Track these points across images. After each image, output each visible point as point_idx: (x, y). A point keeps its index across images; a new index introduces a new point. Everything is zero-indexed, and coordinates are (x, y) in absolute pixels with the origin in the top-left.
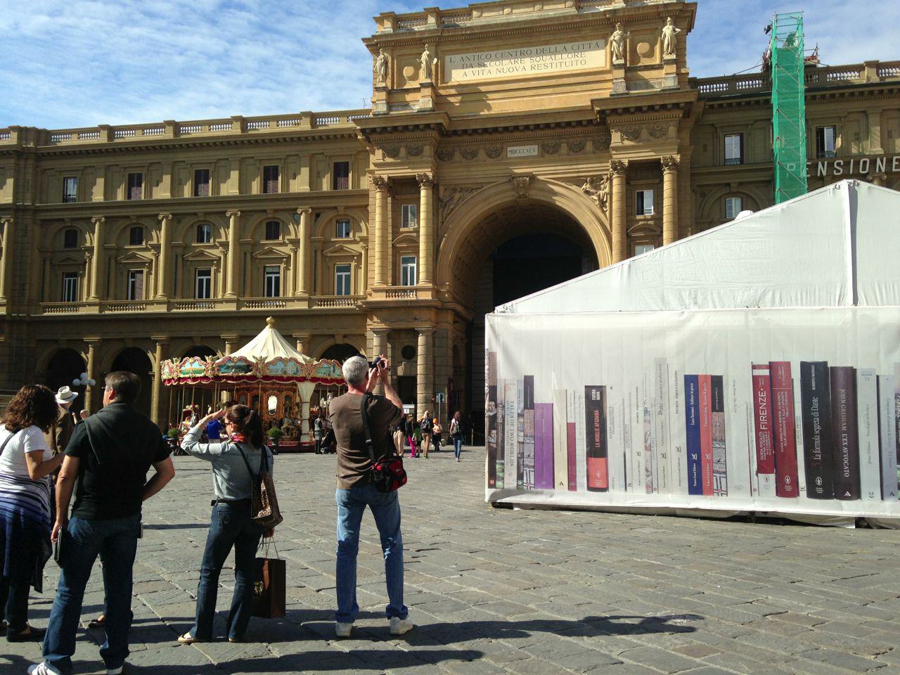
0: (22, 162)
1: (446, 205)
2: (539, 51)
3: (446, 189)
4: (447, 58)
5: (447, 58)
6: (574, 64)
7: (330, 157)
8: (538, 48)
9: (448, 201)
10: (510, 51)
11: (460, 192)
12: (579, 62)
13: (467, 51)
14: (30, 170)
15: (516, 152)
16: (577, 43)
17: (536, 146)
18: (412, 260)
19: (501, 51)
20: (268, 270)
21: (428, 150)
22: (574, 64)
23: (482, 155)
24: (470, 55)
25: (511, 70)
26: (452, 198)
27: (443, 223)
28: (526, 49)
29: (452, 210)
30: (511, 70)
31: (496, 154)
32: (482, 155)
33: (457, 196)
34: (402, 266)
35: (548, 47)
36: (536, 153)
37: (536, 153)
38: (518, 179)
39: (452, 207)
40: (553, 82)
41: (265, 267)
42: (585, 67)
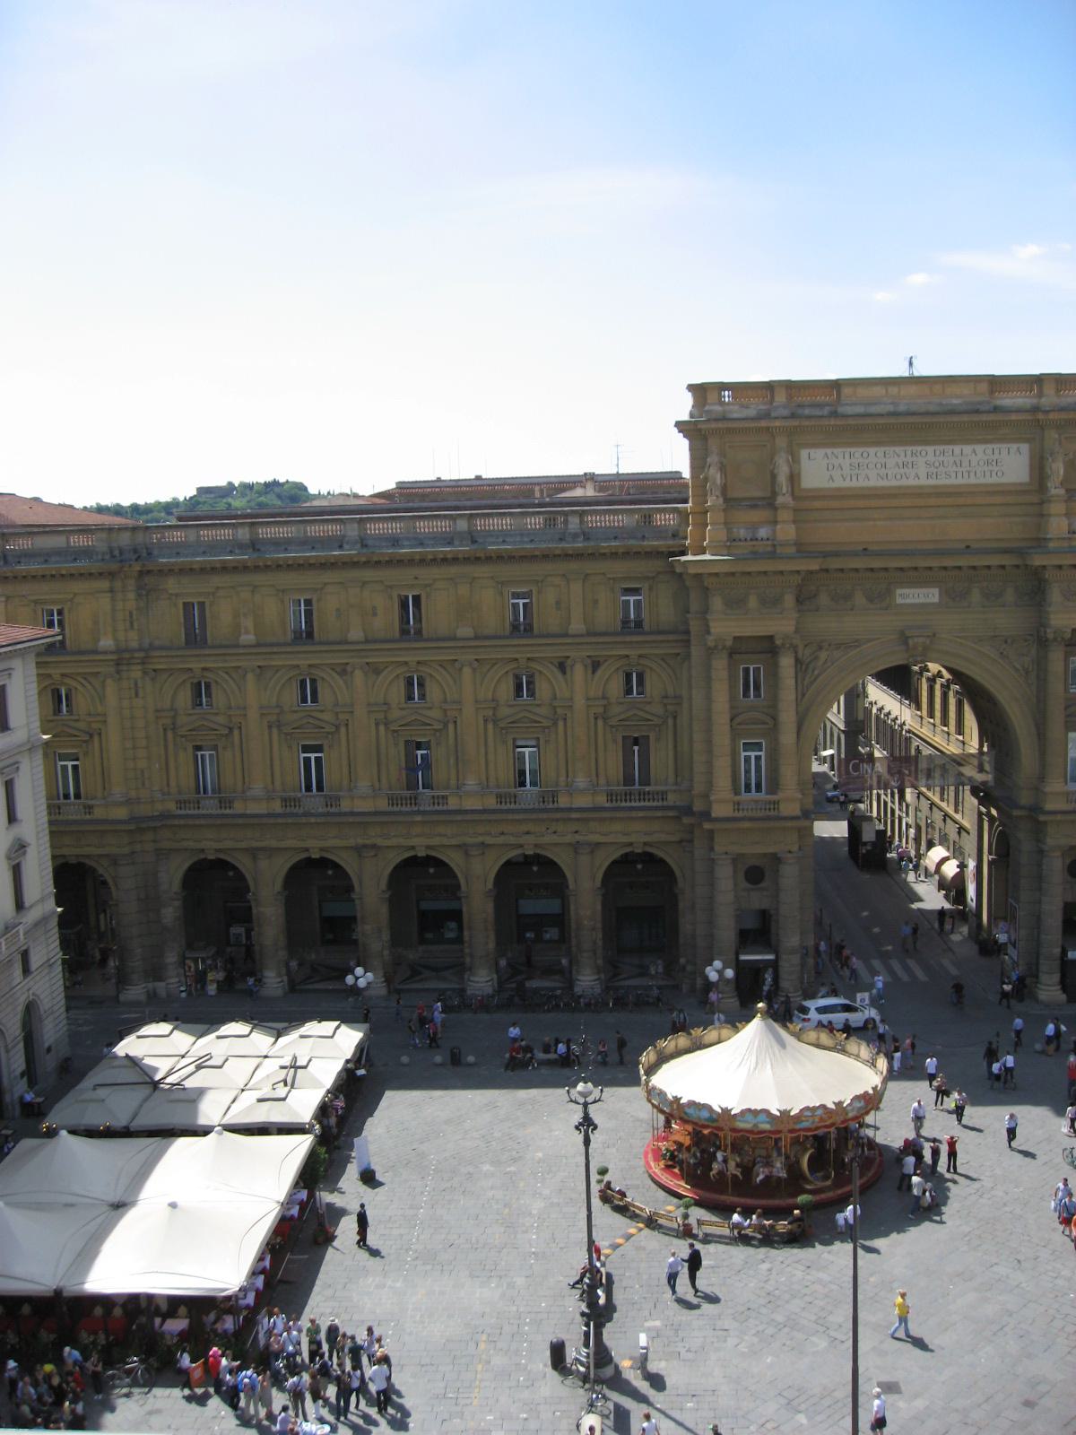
0: (118, 584)
1: (806, 670)
2: (938, 453)
3: (806, 646)
4: (804, 453)
5: (804, 453)
6: (988, 474)
7: (614, 579)
8: (937, 447)
9: (810, 662)
10: (898, 449)
11: (827, 650)
12: (994, 474)
13: (834, 445)
14: (132, 596)
15: (908, 596)
16: (990, 446)
17: (936, 591)
18: (758, 746)
19: (883, 449)
20: (519, 743)
21: (789, 600)
22: (988, 474)
23: (860, 599)
24: (838, 451)
25: (898, 477)
26: (816, 658)
27: (803, 695)
28: (919, 448)
29: (819, 675)
30: (898, 477)
31: (880, 598)
32: (860, 599)
33: (823, 655)
34: (743, 754)
35: (951, 447)
36: (936, 599)
37: (936, 599)
38: (916, 640)
39: (816, 672)
40: (961, 501)
41: (514, 740)
42: (1004, 480)
